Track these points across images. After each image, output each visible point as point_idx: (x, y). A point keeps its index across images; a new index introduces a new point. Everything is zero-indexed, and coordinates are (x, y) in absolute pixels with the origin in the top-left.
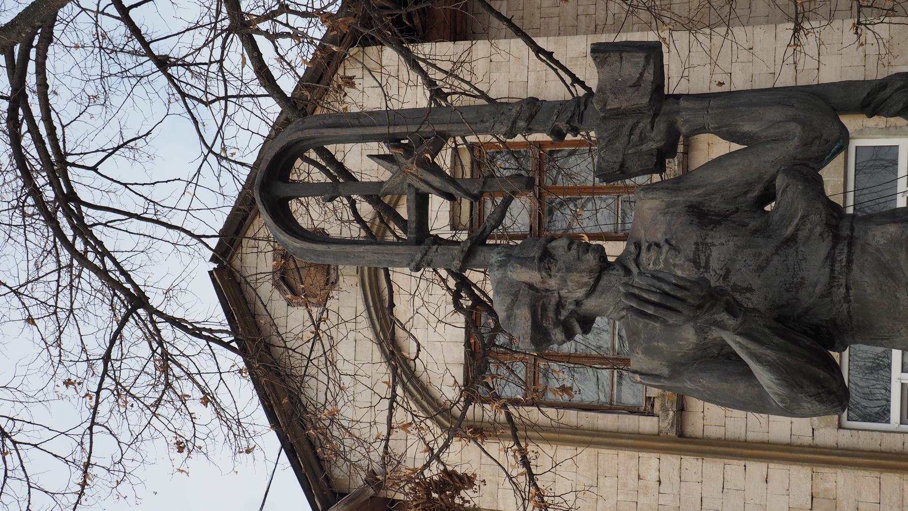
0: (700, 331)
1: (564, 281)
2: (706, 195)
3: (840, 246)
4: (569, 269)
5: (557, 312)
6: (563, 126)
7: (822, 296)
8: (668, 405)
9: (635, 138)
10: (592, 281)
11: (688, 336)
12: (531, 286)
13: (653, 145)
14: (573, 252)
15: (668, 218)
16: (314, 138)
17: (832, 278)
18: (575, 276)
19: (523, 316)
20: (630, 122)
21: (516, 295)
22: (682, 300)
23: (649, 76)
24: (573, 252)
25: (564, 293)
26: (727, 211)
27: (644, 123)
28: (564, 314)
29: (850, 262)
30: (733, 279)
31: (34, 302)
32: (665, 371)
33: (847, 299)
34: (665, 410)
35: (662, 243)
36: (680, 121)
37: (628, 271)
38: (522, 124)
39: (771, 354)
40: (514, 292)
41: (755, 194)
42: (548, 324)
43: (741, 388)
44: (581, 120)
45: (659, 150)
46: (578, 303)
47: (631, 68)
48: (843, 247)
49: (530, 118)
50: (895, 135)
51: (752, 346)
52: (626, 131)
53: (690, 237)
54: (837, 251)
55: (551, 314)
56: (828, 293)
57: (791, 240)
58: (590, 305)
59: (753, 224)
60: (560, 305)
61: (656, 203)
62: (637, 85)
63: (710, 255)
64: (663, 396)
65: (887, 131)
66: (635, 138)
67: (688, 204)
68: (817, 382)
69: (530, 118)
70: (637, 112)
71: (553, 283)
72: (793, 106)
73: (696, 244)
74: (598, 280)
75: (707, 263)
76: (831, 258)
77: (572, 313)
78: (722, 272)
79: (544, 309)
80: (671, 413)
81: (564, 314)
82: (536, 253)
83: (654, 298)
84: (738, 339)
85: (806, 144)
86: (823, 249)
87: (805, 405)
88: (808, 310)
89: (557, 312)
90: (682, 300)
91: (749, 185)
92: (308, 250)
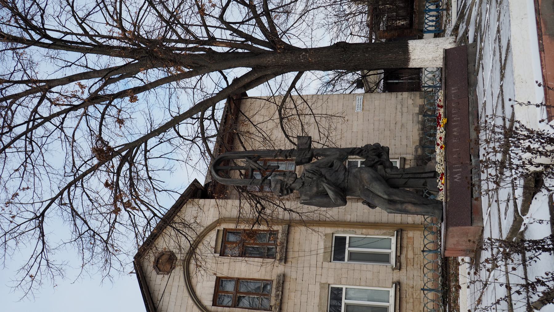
0: (318, 186)
1: (288, 179)
4: (290, 177)
5: (286, 186)
6: (288, 154)
7: (343, 181)
8: (277, 307)
9: (304, 155)
11: (315, 189)
12: (281, 180)
13: (308, 157)
14: (291, 174)
16: (227, 157)
17: (345, 177)
18: (291, 178)
19: (279, 186)
20: (304, 152)
21: (277, 181)
22: (317, 173)
23: (309, 142)
24: (291, 174)
25: (288, 182)
27: (307, 152)
28: (287, 187)
29: (348, 175)
31: (99, 238)
32: (309, 199)
33: (347, 182)
34: (275, 308)
36: (314, 151)
37: (302, 179)
38: (279, 154)
39: (333, 188)
40: (277, 182)
41: (329, 165)
42: (284, 189)
43: (325, 200)
44: (292, 153)
45: (309, 158)
46: (291, 185)
47: (305, 141)
49: (281, 153)
50: (345, 233)
51: (329, 186)
52: (303, 153)
55: (285, 186)
56: (344, 181)
57: (337, 171)
58: (293, 185)
60: (287, 185)
61: (309, 166)
62: (306, 144)
64: (275, 304)
65: (344, 232)
66: (304, 155)
68: (341, 195)
69: (281, 153)
70: (305, 149)
71: (286, 180)
74: (295, 180)
76: (345, 174)
77: (289, 187)
79: (283, 185)
80: (278, 309)
81: (287, 187)
82: (283, 173)
83: (311, 172)
84: (327, 185)
85: (340, 156)
86: (343, 172)
87: (339, 201)
88: (340, 184)
89: (286, 186)
90: (317, 173)
91: (328, 162)
92: (223, 180)
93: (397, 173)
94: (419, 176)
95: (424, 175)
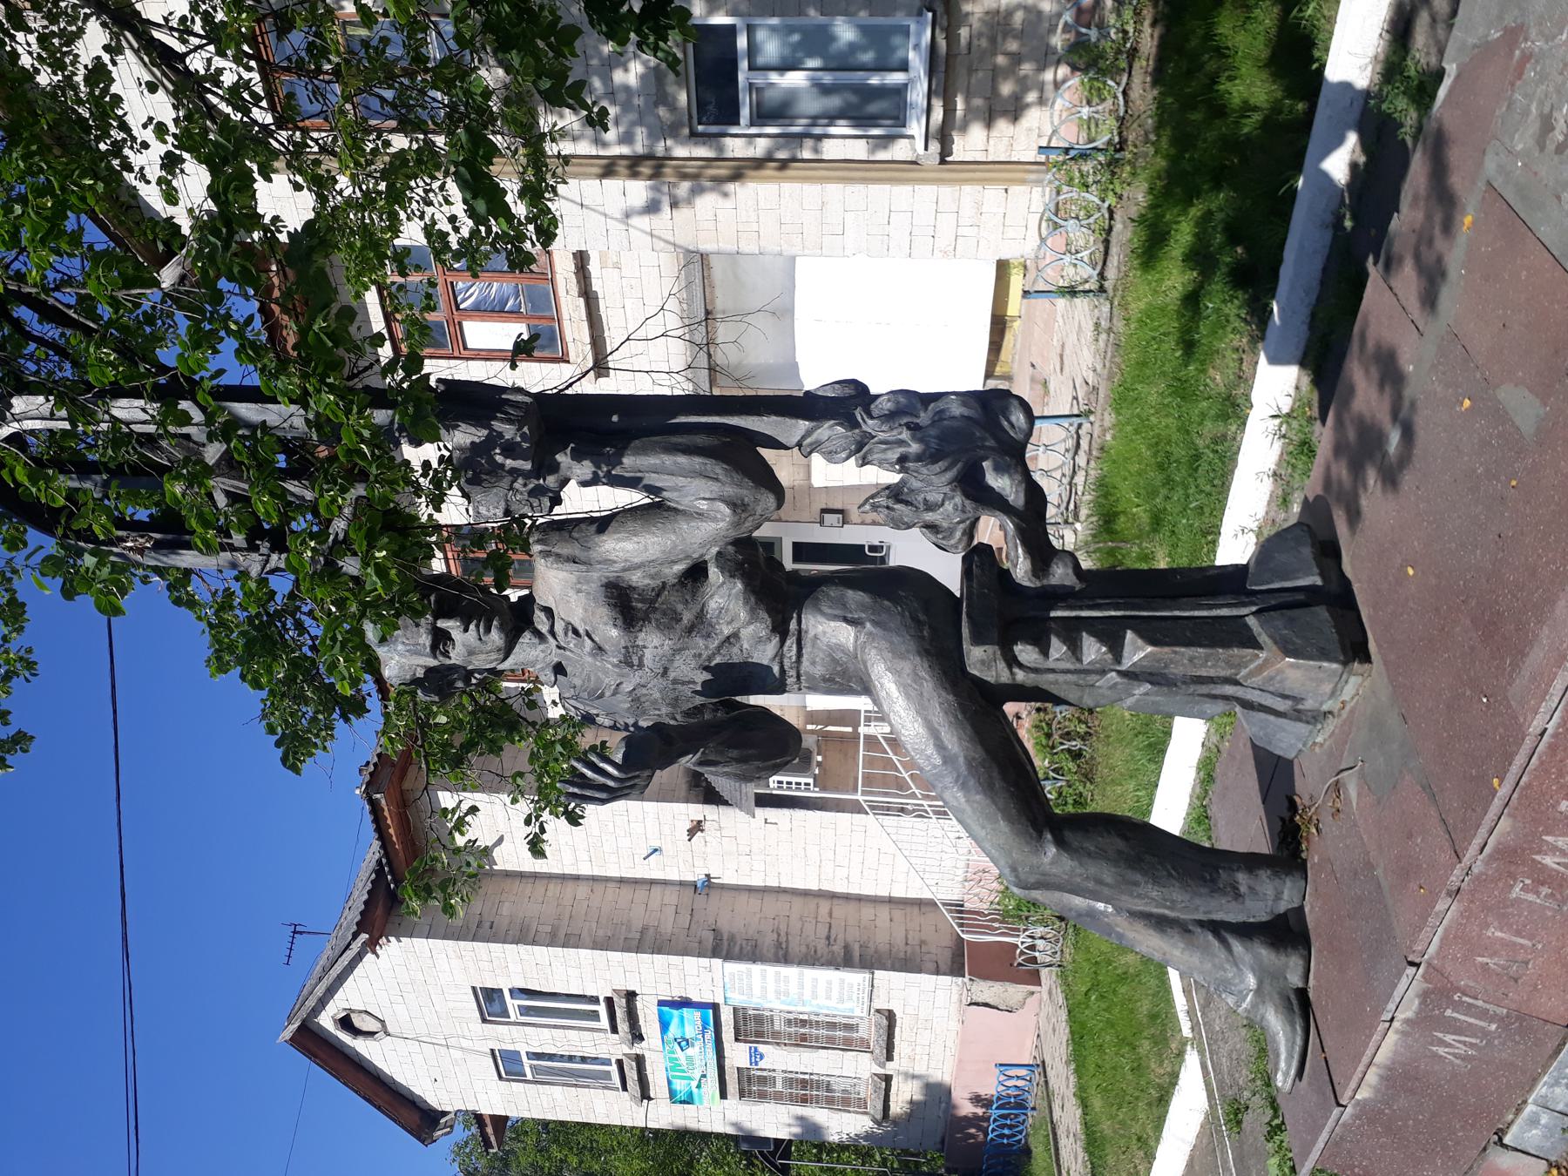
2: (624, 570)
3: (788, 643)
10: (502, 656)
15: (584, 600)
26: (653, 589)
30: (672, 675)
35: (581, 631)
48: (791, 642)
53: (612, 634)
54: (785, 649)
59: (687, 617)
63: (643, 656)
67: (605, 580)
72: (717, 480)
73: (626, 648)
75: (641, 659)
78: (661, 671)
93: (1078, 666)
94: (1204, 689)
95: (1229, 690)
